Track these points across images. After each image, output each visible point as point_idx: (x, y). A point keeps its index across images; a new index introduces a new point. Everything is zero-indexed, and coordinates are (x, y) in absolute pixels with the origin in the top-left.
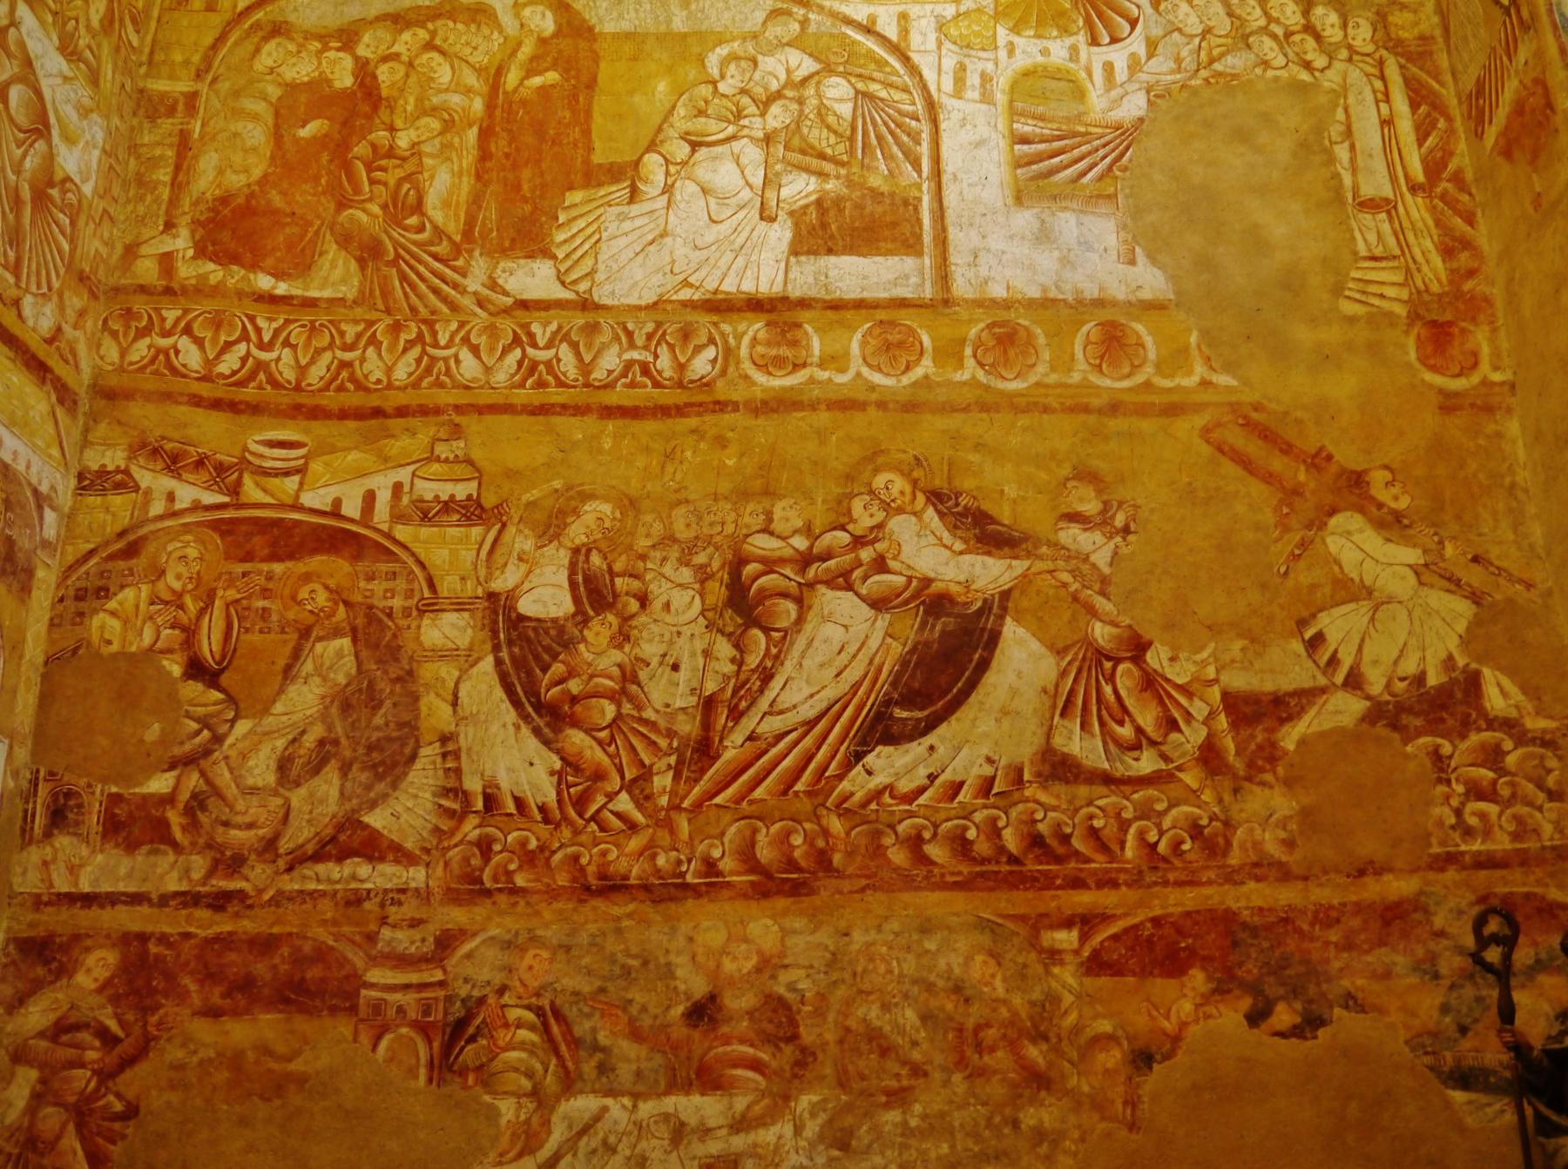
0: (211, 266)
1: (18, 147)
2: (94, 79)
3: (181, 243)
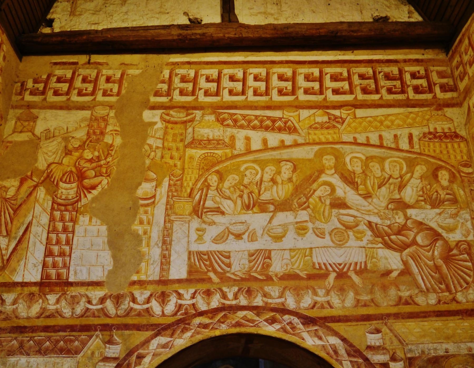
1: (429, 252)
2: (454, 201)
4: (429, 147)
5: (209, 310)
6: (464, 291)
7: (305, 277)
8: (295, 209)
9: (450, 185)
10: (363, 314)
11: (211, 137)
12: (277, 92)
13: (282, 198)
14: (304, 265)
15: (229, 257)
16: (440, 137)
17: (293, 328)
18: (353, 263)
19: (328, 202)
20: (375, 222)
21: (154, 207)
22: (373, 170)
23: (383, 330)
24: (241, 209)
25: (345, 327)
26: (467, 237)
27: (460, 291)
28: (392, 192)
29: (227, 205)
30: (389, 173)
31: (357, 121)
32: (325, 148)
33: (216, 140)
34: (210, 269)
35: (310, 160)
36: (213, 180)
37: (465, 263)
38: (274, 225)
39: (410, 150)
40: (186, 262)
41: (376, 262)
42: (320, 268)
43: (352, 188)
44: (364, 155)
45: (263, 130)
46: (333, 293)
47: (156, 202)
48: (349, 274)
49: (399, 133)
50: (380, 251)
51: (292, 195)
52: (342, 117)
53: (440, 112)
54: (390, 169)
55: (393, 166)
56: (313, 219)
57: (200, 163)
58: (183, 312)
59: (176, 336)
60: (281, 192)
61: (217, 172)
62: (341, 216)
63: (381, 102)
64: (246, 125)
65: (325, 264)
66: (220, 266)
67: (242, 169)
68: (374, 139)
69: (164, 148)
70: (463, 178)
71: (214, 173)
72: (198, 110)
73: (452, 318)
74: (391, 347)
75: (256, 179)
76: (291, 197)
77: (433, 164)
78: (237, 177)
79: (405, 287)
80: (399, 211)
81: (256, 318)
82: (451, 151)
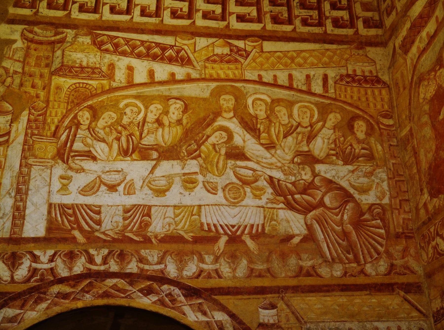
0: (435, 200)
2: (370, 157)
3: (426, 196)
4: (346, 92)
5: (71, 276)
6: (375, 262)
7: (191, 239)
8: (183, 157)
9: (366, 138)
10: (256, 285)
11: (84, 64)
12: (169, 13)
13: (169, 143)
14: (191, 225)
15: (99, 213)
16: (359, 80)
17: (173, 301)
18: (249, 225)
19: (223, 151)
20: (277, 177)
21: (8, 146)
22: (279, 116)
23: (278, 305)
24: (118, 154)
25: (235, 301)
26: (381, 200)
27: (370, 262)
28: (299, 143)
29: (100, 149)
30: (298, 120)
31: (264, 55)
32: (224, 85)
33: (91, 68)
34: (75, 226)
35: (204, 99)
36: (85, 117)
37: (378, 230)
38: (157, 175)
39: (324, 94)
40: (45, 217)
41: (276, 225)
42: (210, 229)
43: (253, 136)
44: (269, 97)
45: (150, 59)
46: (222, 260)
47: (11, 141)
48: (243, 238)
49: (312, 73)
50: (281, 211)
51: (181, 140)
52: (247, 49)
53: (361, 52)
54: (299, 115)
55: (303, 112)
56: (204, 170)
57: (69, 95)
58: (38, 278)
59: (27, 307)
60: (167, 136)
61: (90, 107)
62: (238, 169)
63: (293, 35)
64: (129, 51)
65: (215, 225)
66: (87, 223)
67: (121, 105)
68: (283, 78)
69: (24, 73)
70: (382, 131)
71: (86, 109)
72: (70, 28)
73: (358, 293)
74: (287, 326)
75: (138, 119)
76: (180, 143)
77: (349, 112)
78: (114, 115)
79: (307, 255)
80: (306, 166)
81: (129, 288)
82: (371, 99)
